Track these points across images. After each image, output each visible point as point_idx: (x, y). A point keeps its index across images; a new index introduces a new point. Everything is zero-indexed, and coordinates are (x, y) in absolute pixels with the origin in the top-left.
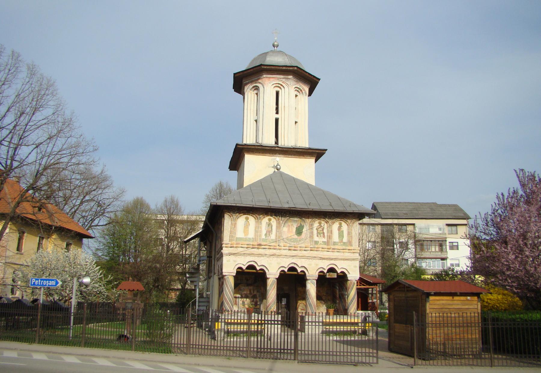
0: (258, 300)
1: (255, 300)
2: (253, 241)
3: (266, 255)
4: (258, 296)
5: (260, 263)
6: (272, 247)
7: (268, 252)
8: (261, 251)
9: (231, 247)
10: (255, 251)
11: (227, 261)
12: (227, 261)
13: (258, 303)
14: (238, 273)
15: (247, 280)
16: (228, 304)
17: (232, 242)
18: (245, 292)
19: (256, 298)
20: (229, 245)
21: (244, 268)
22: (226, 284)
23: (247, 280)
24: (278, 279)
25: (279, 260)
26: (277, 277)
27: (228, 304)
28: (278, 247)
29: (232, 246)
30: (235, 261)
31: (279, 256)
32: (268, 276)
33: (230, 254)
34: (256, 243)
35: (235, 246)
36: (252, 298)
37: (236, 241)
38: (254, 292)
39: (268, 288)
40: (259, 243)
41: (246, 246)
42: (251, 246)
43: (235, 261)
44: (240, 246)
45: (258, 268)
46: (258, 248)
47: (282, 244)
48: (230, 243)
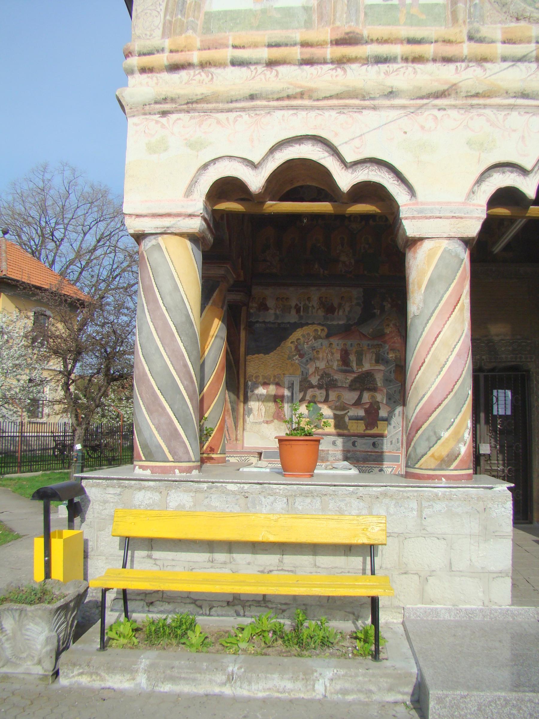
0: (380, 397)
1: (366, 397)
2: (308, 25)
3: (391, 94)
4: (379, 378)
5: (356, 142)
6: (428, 50)
7: (403, 77)
8: (359, 76)
9: (175, 68)
10: (323, 78)
11: (152, 149)
12: (152, 149)
13: (383, 413)
14: (217, 221)
15: (330, 310)
16: (154, 407)
17: (181, 40)
18: (322, 365)
19: (374, 389)
20: (164, 59)
21: (256, 181)
22: (148, 290)
23: (330, 310)
24: (481, 249)
25: (480, 123)
26: (473, 228)
27: (154, 407)
28: (467, 48)
29: (178, 58)
30: (195, 145)
31: (479, 97)
32: (410, 228)
33: (164, 107)
34: (326, 34)
35: (195, 57)
36: (352, 388)
37: (207, 30)
38: (360, 362)
39: (415, 304)
40: (344, 26)
41: (265, 54)
42: (297, 53)
43: (195, 145)
44: (229, 53)
45: (345, 180)
46: (340, 62)
47: (493, 30)
48: (167, 44)
